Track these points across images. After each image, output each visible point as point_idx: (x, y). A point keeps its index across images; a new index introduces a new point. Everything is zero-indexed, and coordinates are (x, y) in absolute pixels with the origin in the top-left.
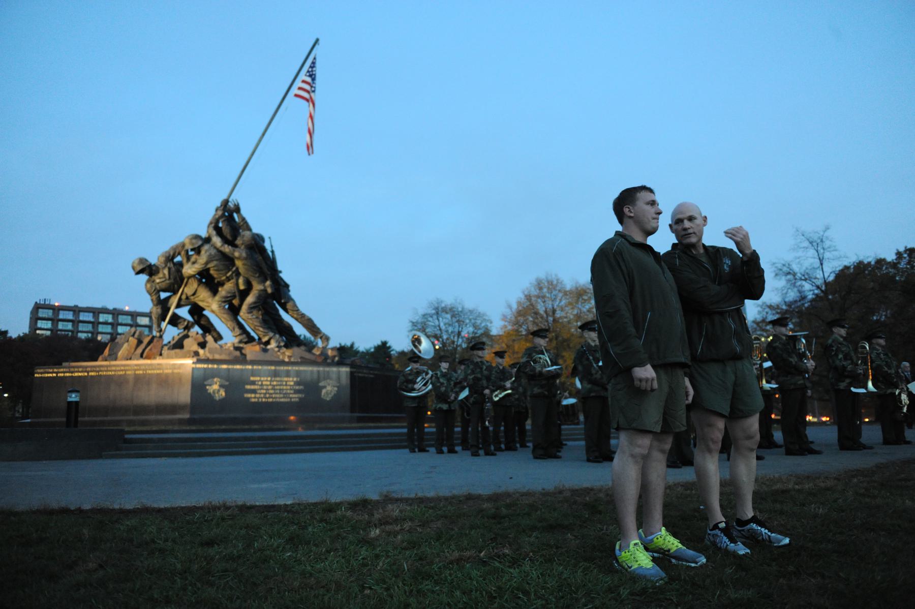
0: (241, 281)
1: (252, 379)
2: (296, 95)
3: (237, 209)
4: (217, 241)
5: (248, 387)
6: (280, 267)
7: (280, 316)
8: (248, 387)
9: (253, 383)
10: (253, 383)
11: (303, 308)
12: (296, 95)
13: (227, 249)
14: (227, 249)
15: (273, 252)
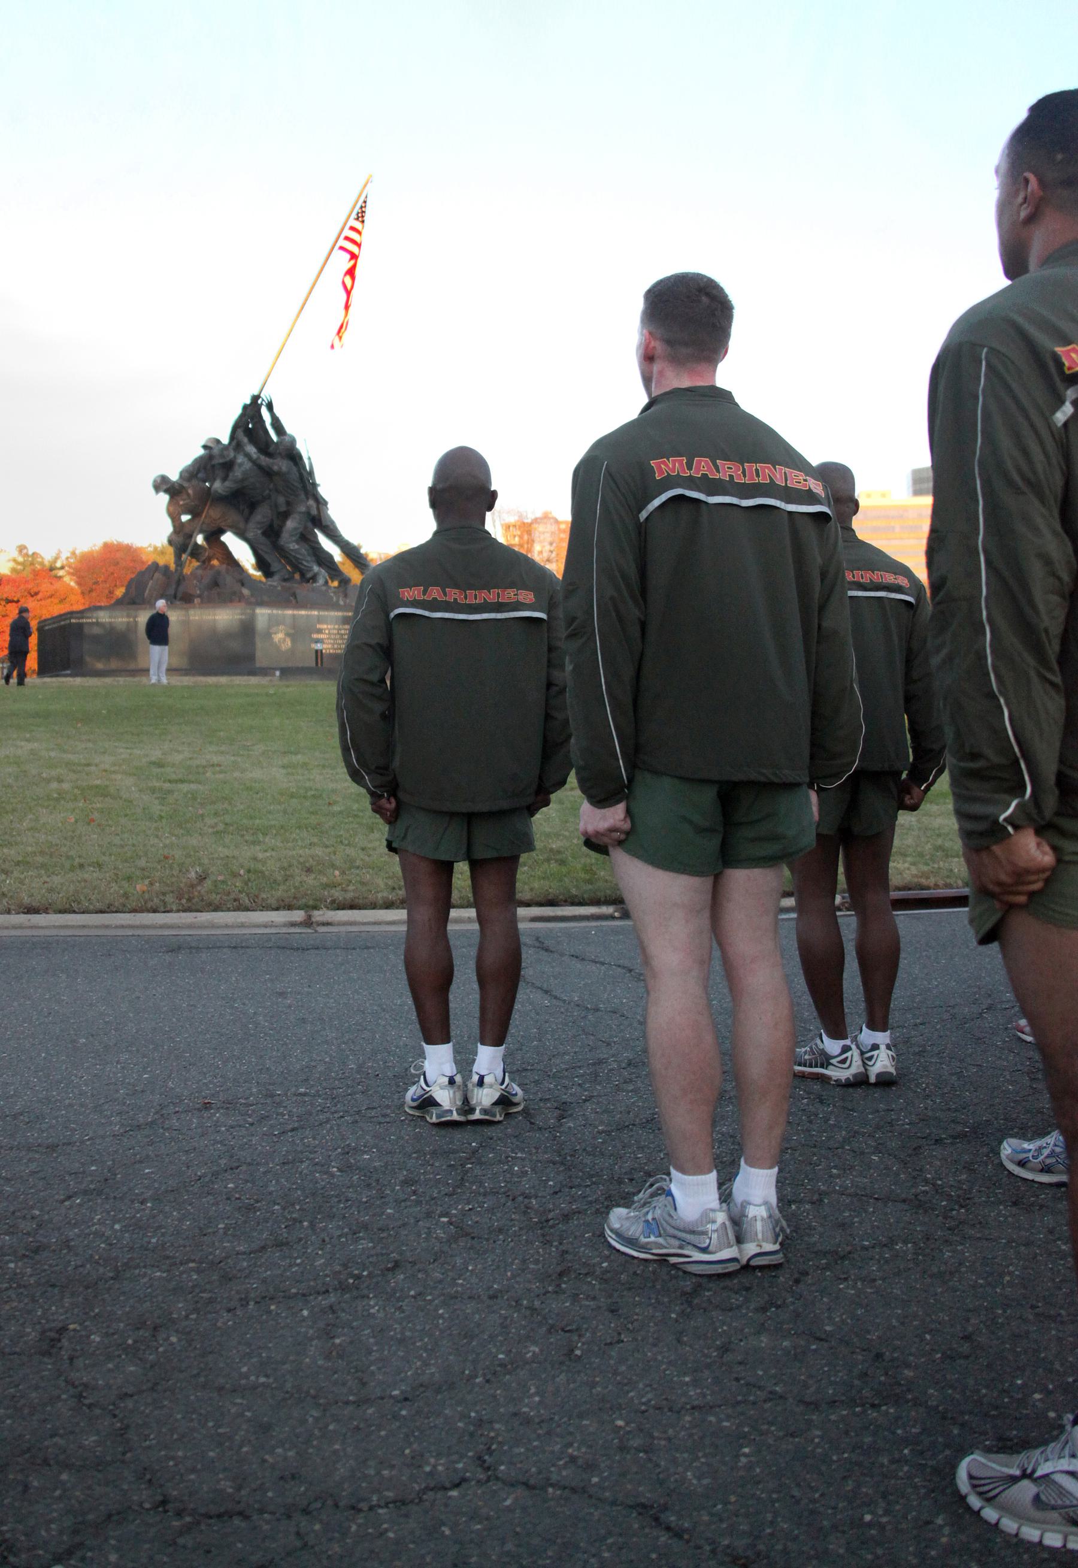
0: (281, 500)
1: (318, 626)
2: (341, 248)
3: (270, 406)
4: (251, 449)
5: (315, 636)
6: (319, 478)
7: (319, 543)
8: (315, 636)
9: (320, 631)
10: (320, 631)
11: (348, 534)
12: (341, 248)
13: (264, 460)
14: (264, 460)
15: (309, 458)
